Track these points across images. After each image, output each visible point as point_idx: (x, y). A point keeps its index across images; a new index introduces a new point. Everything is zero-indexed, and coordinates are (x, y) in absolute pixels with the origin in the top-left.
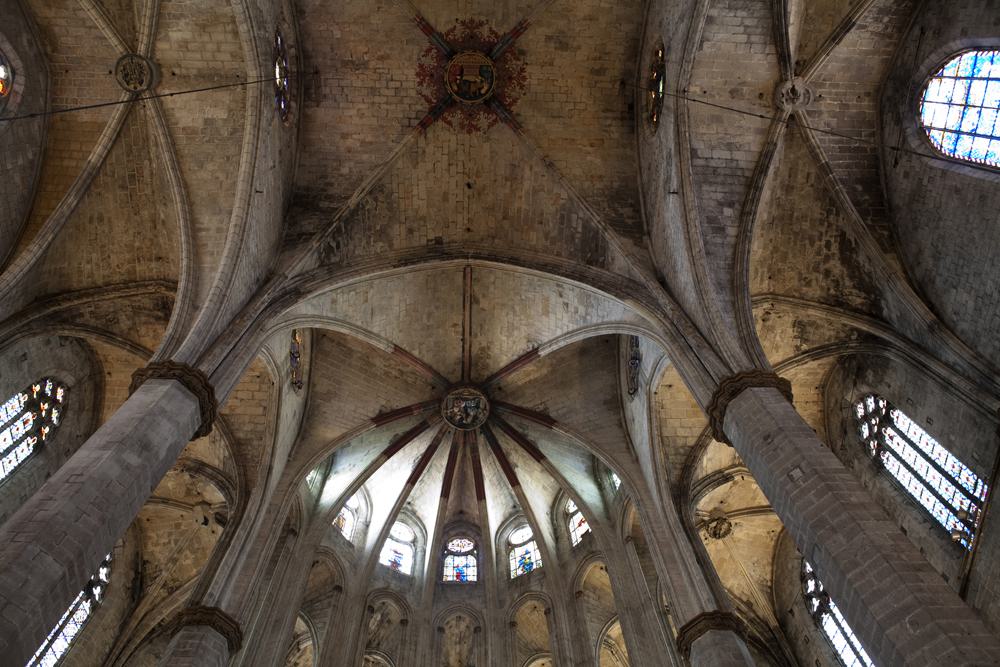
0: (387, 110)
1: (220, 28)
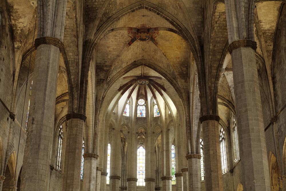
0: (120, 40)
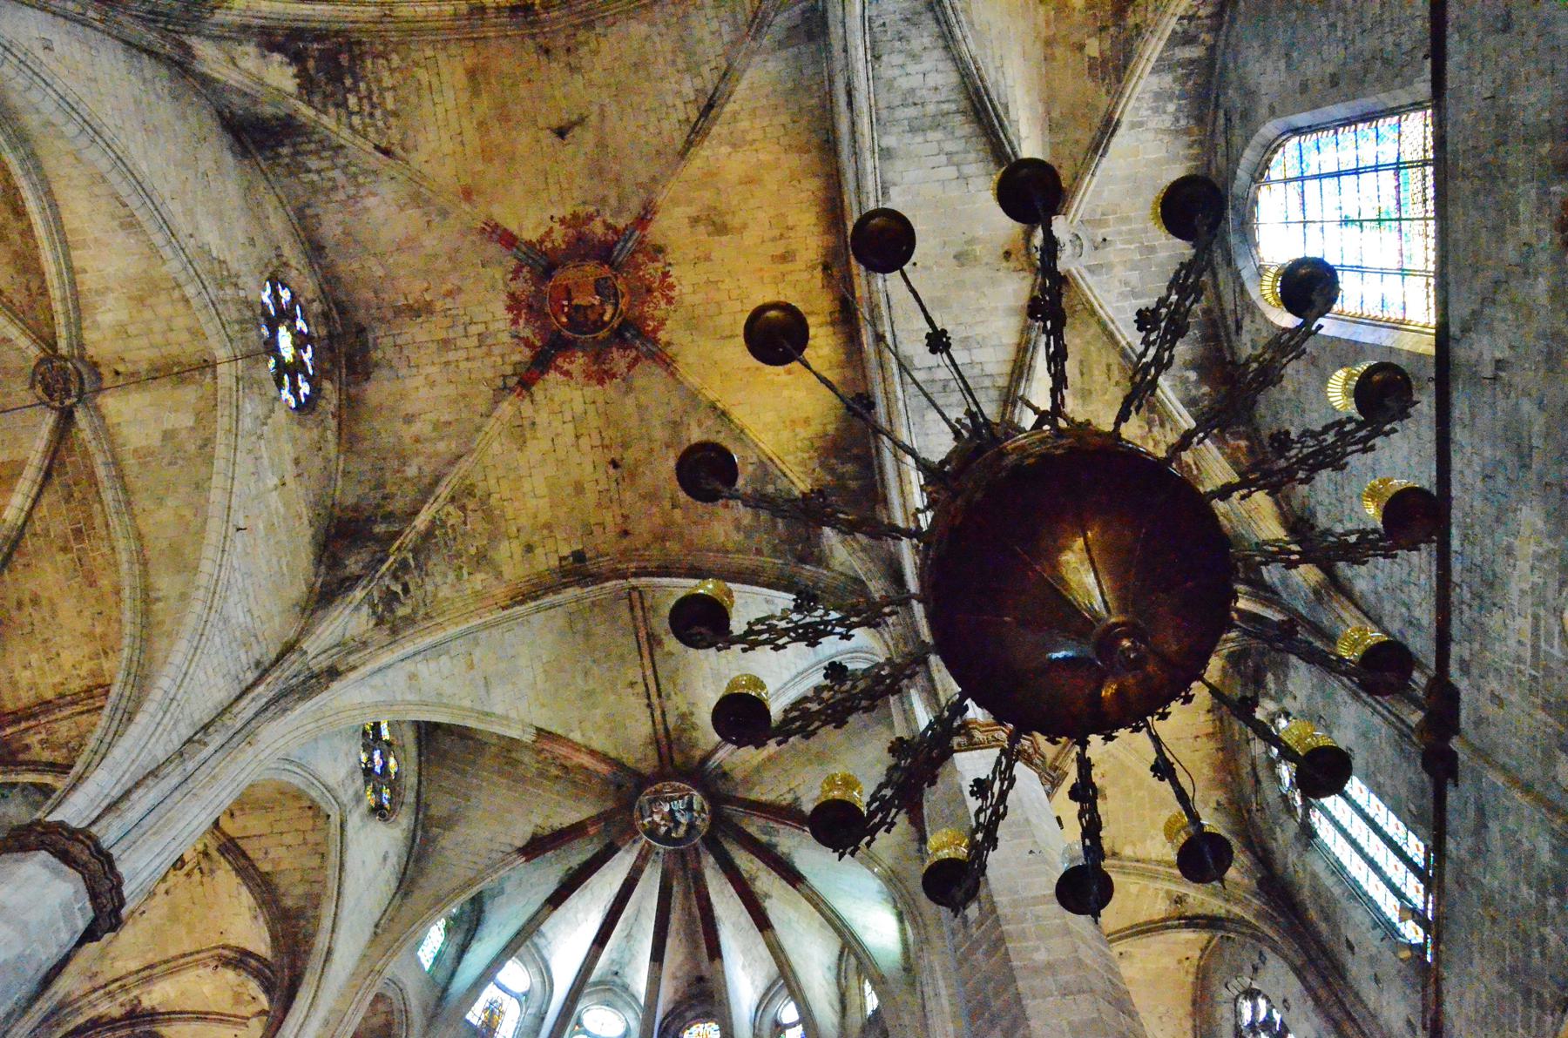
1: (163, 297)
